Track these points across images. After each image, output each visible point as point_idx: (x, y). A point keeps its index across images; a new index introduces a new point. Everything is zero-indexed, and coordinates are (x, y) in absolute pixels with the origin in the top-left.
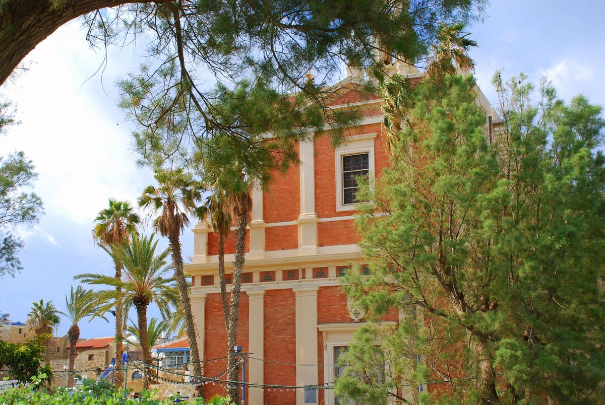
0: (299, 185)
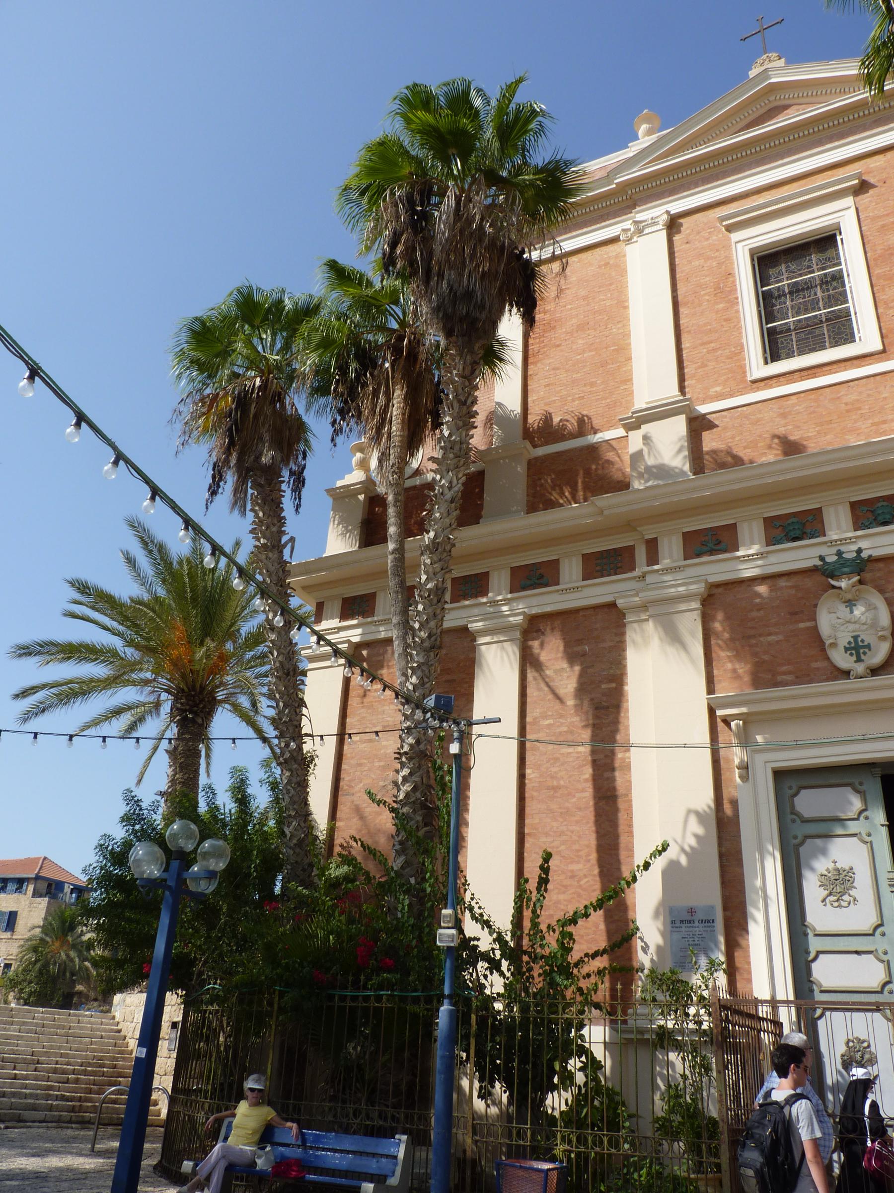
0: (629, 344)
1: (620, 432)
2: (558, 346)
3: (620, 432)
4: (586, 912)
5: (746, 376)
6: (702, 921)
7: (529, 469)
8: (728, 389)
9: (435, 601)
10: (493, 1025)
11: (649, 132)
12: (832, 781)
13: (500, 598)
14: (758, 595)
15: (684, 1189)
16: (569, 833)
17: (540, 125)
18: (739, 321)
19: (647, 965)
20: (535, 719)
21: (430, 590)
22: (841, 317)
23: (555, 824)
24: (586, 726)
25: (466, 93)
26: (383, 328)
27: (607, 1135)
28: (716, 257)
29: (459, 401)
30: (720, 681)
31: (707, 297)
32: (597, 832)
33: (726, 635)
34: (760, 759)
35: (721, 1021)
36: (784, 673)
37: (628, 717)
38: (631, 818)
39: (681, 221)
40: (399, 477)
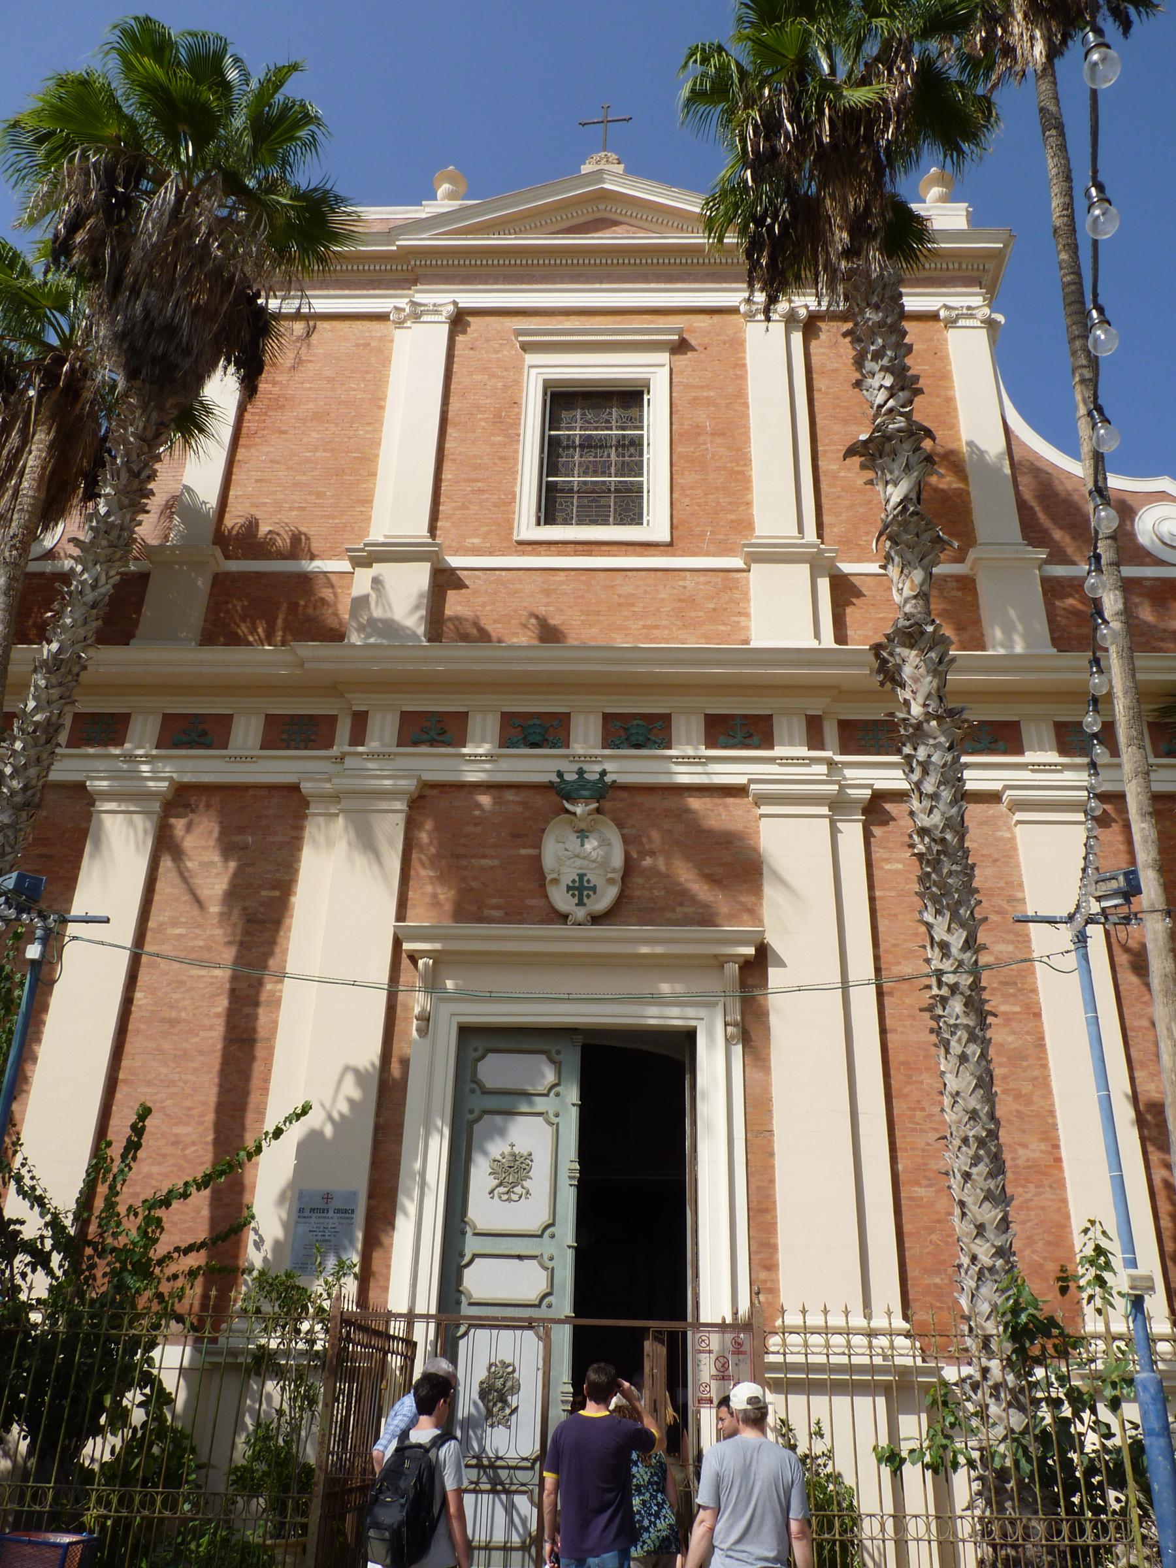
0: (377, 456)
1: (345, 565)
2: (284, 432)
3: (345, 565)
4: (185, 1191)
5: (512, 534)
6: (338, 1211)
7: (213, 586)
8: (488, 545)
9: (43, 739)
10: (23, 1343)
11: (451, 196)
12: (526, 1047)
13: (140, 752)
14: (479, 806)
15: (255, 1560)
16: (181, 1084)
17: (313, 137)
18: (516, 464)
19: (258, 1264)
20: (161, 924)
21: (37, 724)
22: (631, 491)
23: (163, 1070)
24: (229, 943)
25: (219, 57)
26: (35, 339)
27: (162, 1493)
28: (503, 377)
29: (130, 471)
30: (414, 906)
31: (483, 424)
32: (220, 1086)
33: (433, 850)
34: (446, 1009)
35: (340, 1339)
36: (493, 908)
37: (288, 938)
38: (270, 1070)
39: (470, 319)
40: (20, 555)
